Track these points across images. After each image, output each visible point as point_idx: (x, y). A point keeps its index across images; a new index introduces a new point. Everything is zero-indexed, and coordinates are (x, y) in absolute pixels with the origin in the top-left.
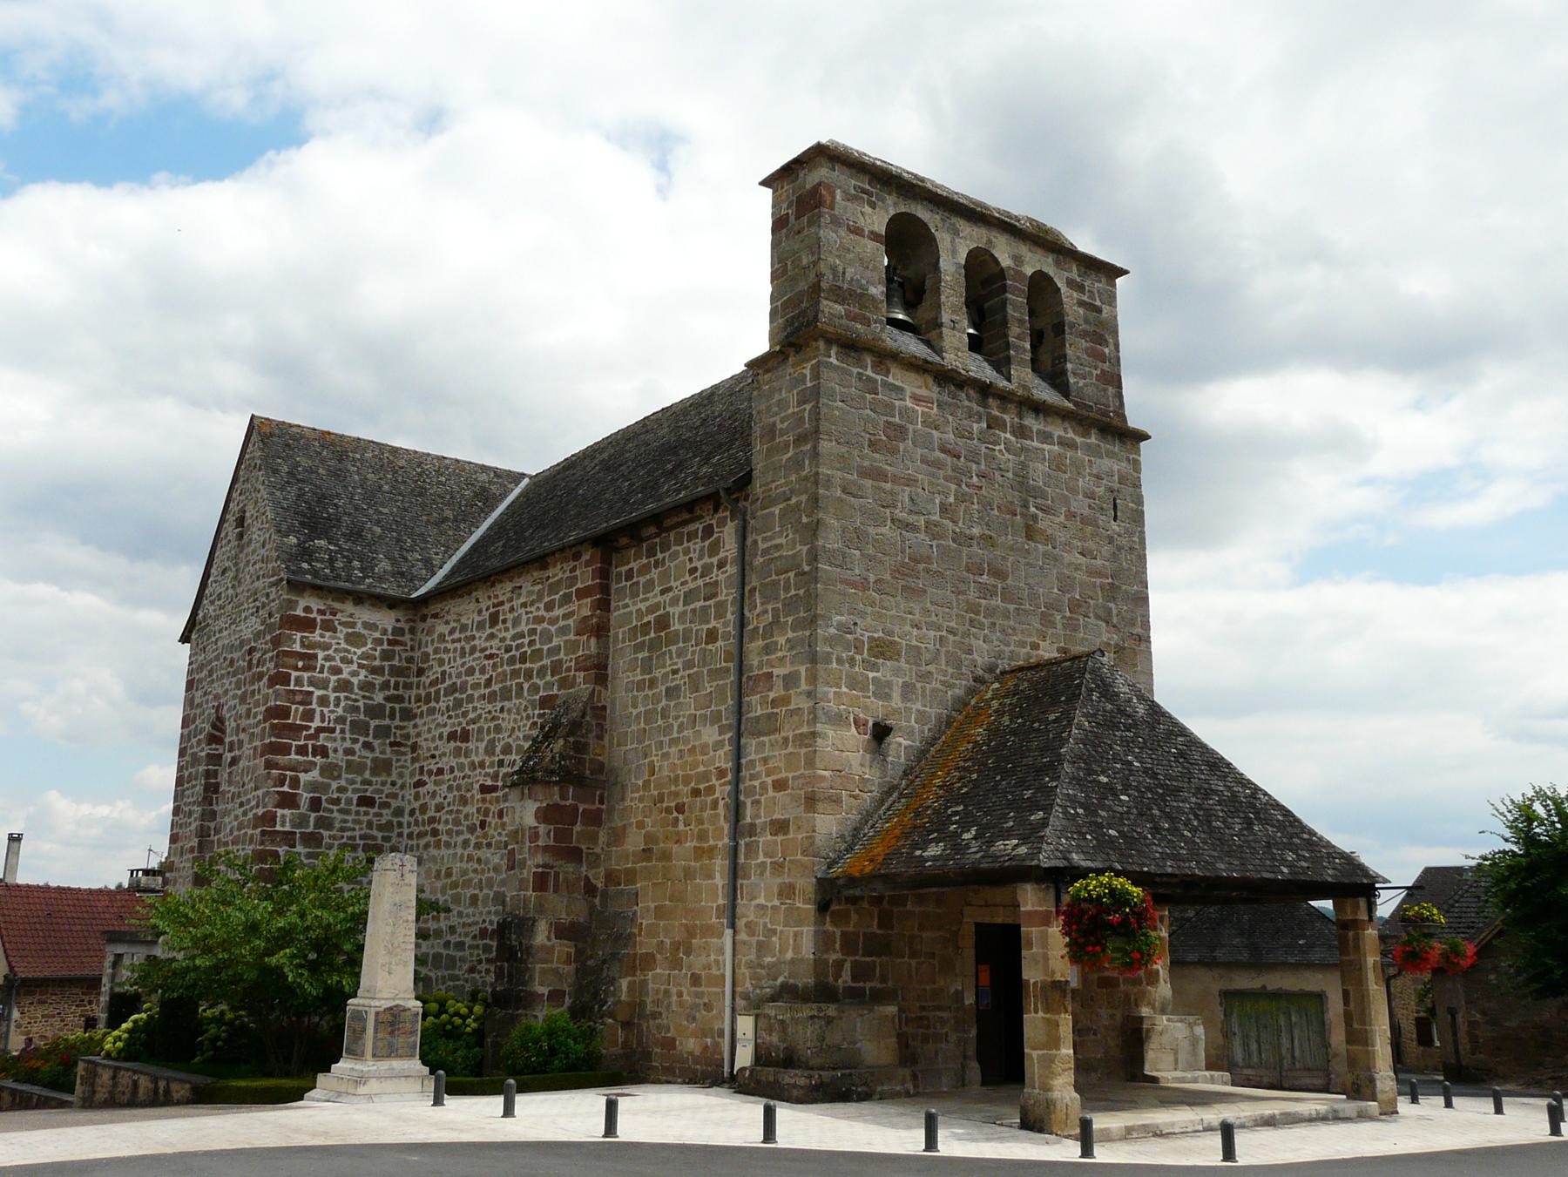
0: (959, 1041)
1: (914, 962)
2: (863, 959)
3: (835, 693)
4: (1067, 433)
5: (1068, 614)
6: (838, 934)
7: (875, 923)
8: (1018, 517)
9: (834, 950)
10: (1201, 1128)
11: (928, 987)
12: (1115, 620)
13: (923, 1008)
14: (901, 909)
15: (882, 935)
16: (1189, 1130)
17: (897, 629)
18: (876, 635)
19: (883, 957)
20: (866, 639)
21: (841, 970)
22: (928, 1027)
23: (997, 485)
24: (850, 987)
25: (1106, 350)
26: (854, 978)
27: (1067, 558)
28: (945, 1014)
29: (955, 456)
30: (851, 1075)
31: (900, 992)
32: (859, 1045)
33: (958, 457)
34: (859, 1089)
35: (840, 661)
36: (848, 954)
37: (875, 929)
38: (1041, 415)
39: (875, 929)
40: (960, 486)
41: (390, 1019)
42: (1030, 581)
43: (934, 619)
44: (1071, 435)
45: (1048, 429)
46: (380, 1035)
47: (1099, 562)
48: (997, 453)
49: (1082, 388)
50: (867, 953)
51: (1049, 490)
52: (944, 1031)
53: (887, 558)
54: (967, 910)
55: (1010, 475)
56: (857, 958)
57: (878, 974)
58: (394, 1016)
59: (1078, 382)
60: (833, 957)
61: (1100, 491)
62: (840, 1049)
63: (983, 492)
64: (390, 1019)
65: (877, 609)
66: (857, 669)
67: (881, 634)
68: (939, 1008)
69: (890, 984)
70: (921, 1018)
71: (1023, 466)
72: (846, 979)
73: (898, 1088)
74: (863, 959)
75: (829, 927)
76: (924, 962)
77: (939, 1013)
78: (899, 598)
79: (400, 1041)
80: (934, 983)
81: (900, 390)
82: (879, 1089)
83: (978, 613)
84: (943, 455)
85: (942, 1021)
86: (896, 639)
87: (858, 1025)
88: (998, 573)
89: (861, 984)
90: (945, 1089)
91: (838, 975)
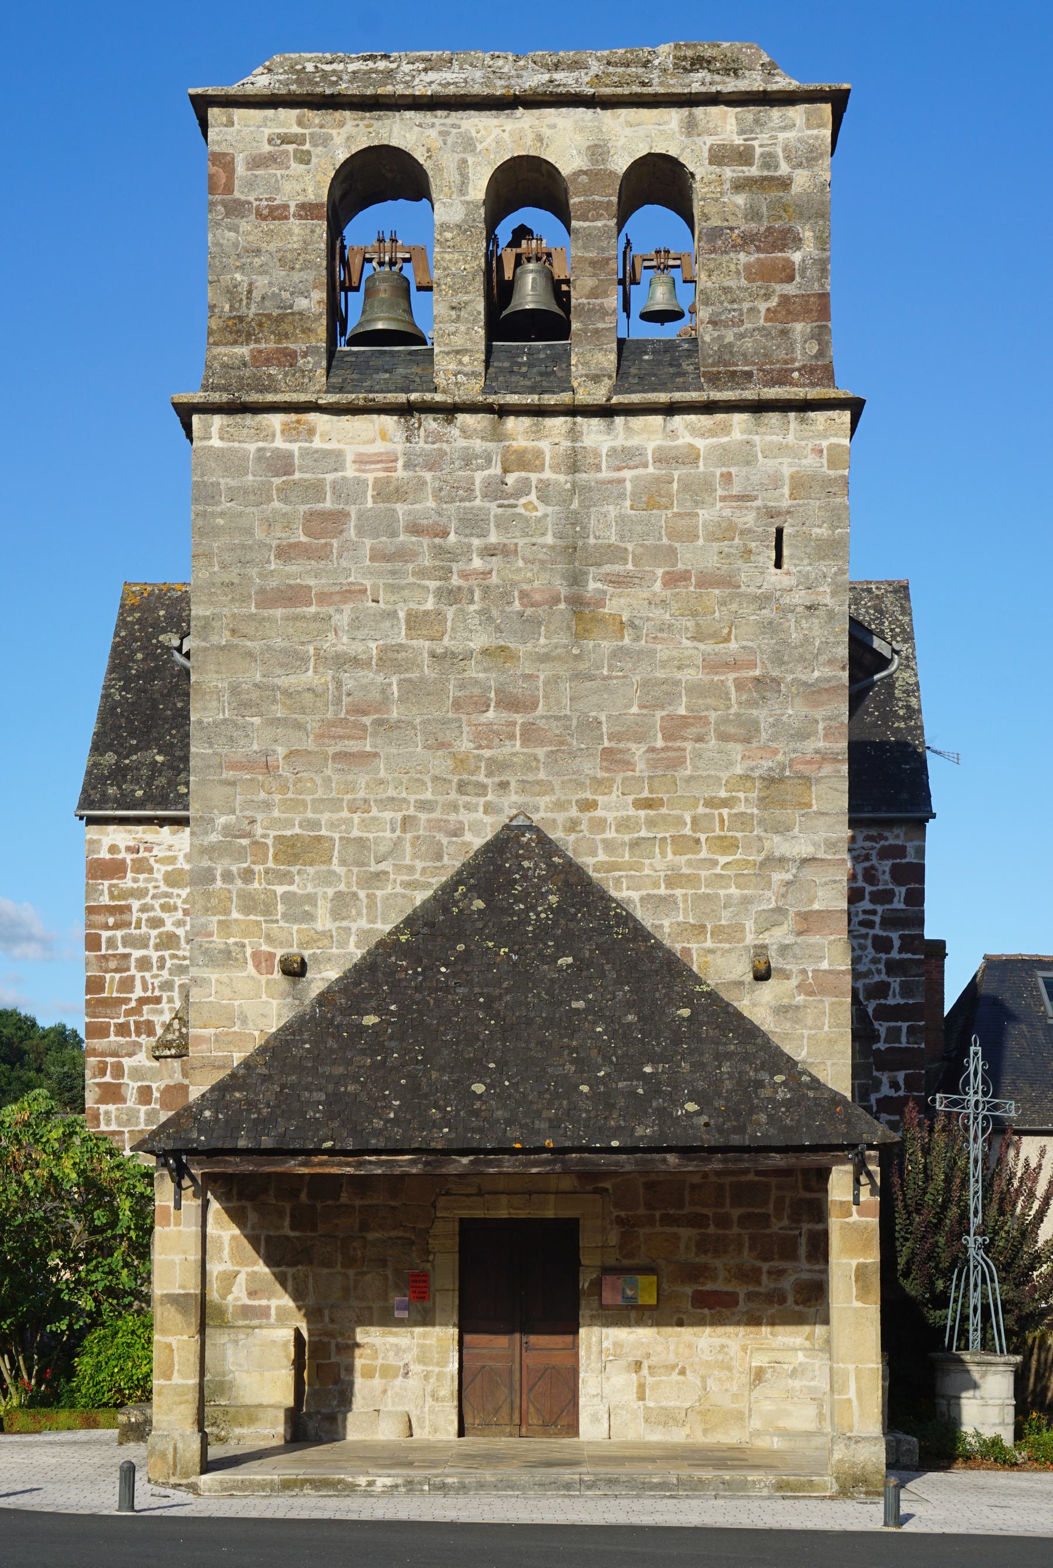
5: (660, 743)
20: (270, 842)
27: (663, 652)
35: (228, 877)
43: (391, 792)
54: (442, 1201)
55: (549, 539)
63: (494, 579)
65: (290, 795)
66: (256, 885)
67: (297, 830)
71: (574, 520)
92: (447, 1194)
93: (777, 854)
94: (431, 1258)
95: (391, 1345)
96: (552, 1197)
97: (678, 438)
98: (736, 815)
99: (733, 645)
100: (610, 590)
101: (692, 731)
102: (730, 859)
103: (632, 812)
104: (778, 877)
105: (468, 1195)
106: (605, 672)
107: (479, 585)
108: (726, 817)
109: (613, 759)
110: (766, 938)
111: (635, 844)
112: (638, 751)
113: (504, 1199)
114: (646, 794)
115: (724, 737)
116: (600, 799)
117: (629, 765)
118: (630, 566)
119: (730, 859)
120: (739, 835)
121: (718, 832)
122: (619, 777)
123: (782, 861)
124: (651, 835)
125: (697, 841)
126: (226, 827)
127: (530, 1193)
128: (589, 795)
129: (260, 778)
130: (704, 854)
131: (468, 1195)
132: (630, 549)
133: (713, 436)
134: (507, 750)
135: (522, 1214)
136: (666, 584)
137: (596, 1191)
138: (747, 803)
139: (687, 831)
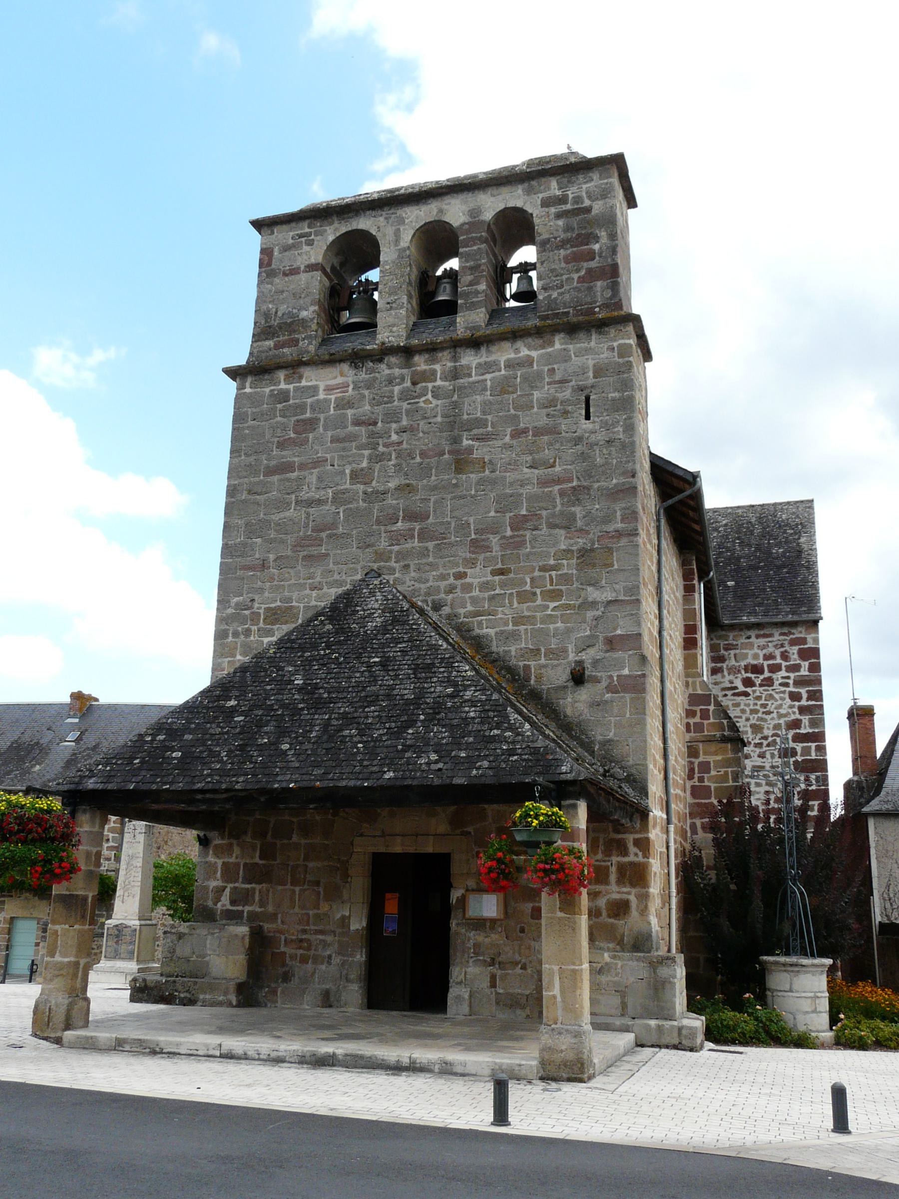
0: (343, 964)
1: (297, 889)
2: (244, 886)
3: (229, 662)
4: (517, 351)
5: (509, 533)
6: (220, 862)
7: (258, 854)
9: (215, 879)
10: (218, 1054)
11: (311, 913)
13: (304, 931)
14: (285, 841)
15: (264, 865)
16: (199, 1053)
17: (295, 595)
18: (273, 605)
19: (264, 885)
20: (262, 611)
21: (221, 896)
22: (309, 949)
23: (421, 435)
24: (228, 910)
25: (596, 247)
26: (233, 902)
27: (510, 476)
28: (329, 938)
29: (370, 424)
30: (174, 982)
31: (280, 916)
32: (207, 959)
34: (182, 995)
35: (236, 634)
36: (227, 881)
37: (257, 860)
39: (257, 860)
40: (375, 449)
41: (116, 932)
42: (456, 513)
43: (336, 577)
44: (525, 352)
45: (492, 358)
46: (110, 943)
48: (422, 405)
49: (556, 299)
50: (247, 880)
51: (489, 417)
52: (328, 953)
53: (289, 537)
54: (357, 840)
55: (439, 419)
56: (237, 885)
57: (257, 898)
58: (118, 930)
59: (550, 296)
60: (213, 884)
61: (567, 394)
62: (189, 961)
63: (405, 446)
64: (116, 932)
65: (276, 583)
66: (252, 638)
67: (279, 603)
68: (322, 932)
69: (270, 909)
70: (301, 941)
71: (455, 405)
72: (225, 902)
73: (221, 998)
74: (244, 886)
75: (211, 859)
76: (306, 890)
77: (321, 937)
78: (299, 567)
79: (123, 948)
80: (319, 909)
81: (315, 389)
82: (201, 997)
83: (389, 559)
84: (357, 428)
85: (325, 944)
86: (294, 604)
87: (208, 942)
89: (240, 908)
90: (307, 1007)
91: (217, 900)
92: (361, 835)
93: (590, 599)
94: (349, 880)
95: (321, 941)
96: (432, 837)
97: (520, 352)
98: (561, 575)
99: (558, 469)
100: (476, 444)
101: (529, 525)
102: (557, 604)
103: (490, 578)
104: (590, 614)
105: (374, 836)
106: (473, 492)
107: (395, 450)
108: (554, 577)
109: (478, 546)
110: (583, 656)
111: (492, 598)
112: (494, 540)
113: (399, 840)
114: (500, 566)
115: (552, 526)
116: (469, 571)
117: (488, 549)
118: (489, 429)
119: (557, 604)
120: (563, 588)
121: (549, 587)
122: (481, 557)
123: (594, 604)
124: (503, 592)
125: (535, 594)
126: (237, 604)
127: (417, 835)
128: (461, 569)
129: (259, 574)
130: (539, 602)
131: (374, 836)
132: (490, 419)
133: (542, 349)
134: (409, 545)
135: (411, 850)
136: (513, 437)
137: (462, 834)
138: (569, 567)
139: (528, 587)
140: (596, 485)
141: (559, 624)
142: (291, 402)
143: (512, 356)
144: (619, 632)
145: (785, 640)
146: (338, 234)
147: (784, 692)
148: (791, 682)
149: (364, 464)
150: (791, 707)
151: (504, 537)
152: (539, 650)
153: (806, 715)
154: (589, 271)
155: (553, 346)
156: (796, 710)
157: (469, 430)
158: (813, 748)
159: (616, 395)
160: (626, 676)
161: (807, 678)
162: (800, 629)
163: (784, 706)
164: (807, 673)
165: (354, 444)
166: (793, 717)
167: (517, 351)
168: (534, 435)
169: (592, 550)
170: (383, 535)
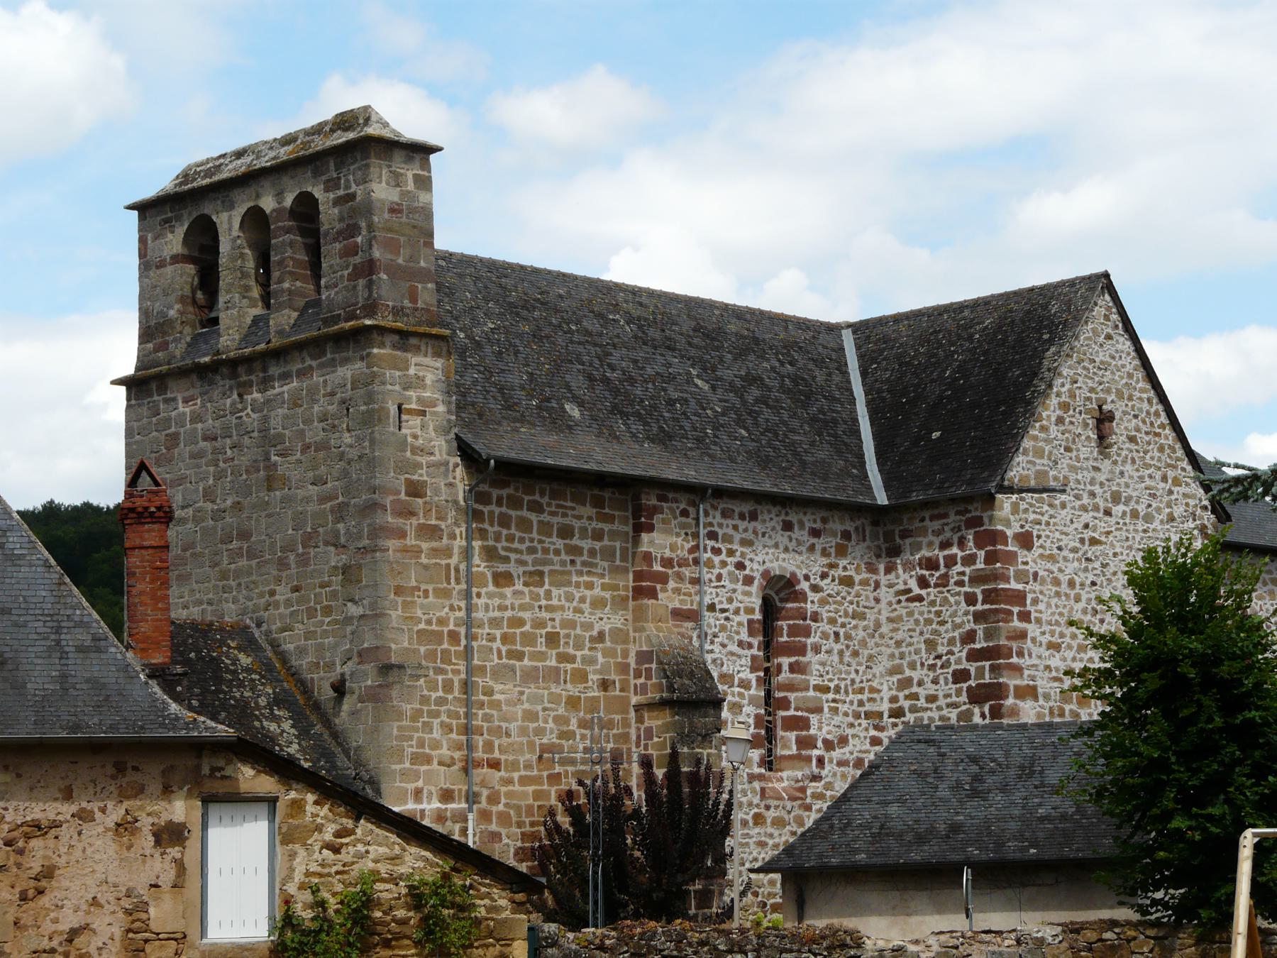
8: (262, 472)
12: (343, 540)
29: (213, 439)
33: (215, 439)
38: (282, 360)
40: (217, 465)
47: (329, 485)
55: (255, 434)
88: (244, 535)
104: (349, 629)
115: (327, 543)
120: (333, 603)
125: (316, 610)
140: (353, 501)
141: (331, 639)
142: (162, 415)
143: (300, 366)
144: (366, 645)
145: (961, 521)
146: (191, 220)
147: (958, 594)
148: (966, 579)
149: (211, 482)
150: (966, 613)
151: (298, 555)
152: (319, 663)
153: (981, 624)
154: (355, 267)
155: (326, 355)
156: (971, 618)
157: (275, 446)
158: (987, 668)
159: (363, 408)
160: (371, 687)
161: (981, 573)
162: (975, 505)
163: (960, 613)
164: (982, 566)
165: (203, 460)
166: (968, 627)
167: (303, 361)
168: (315, 451)
169: (350, 567)
170: (225, 553)
